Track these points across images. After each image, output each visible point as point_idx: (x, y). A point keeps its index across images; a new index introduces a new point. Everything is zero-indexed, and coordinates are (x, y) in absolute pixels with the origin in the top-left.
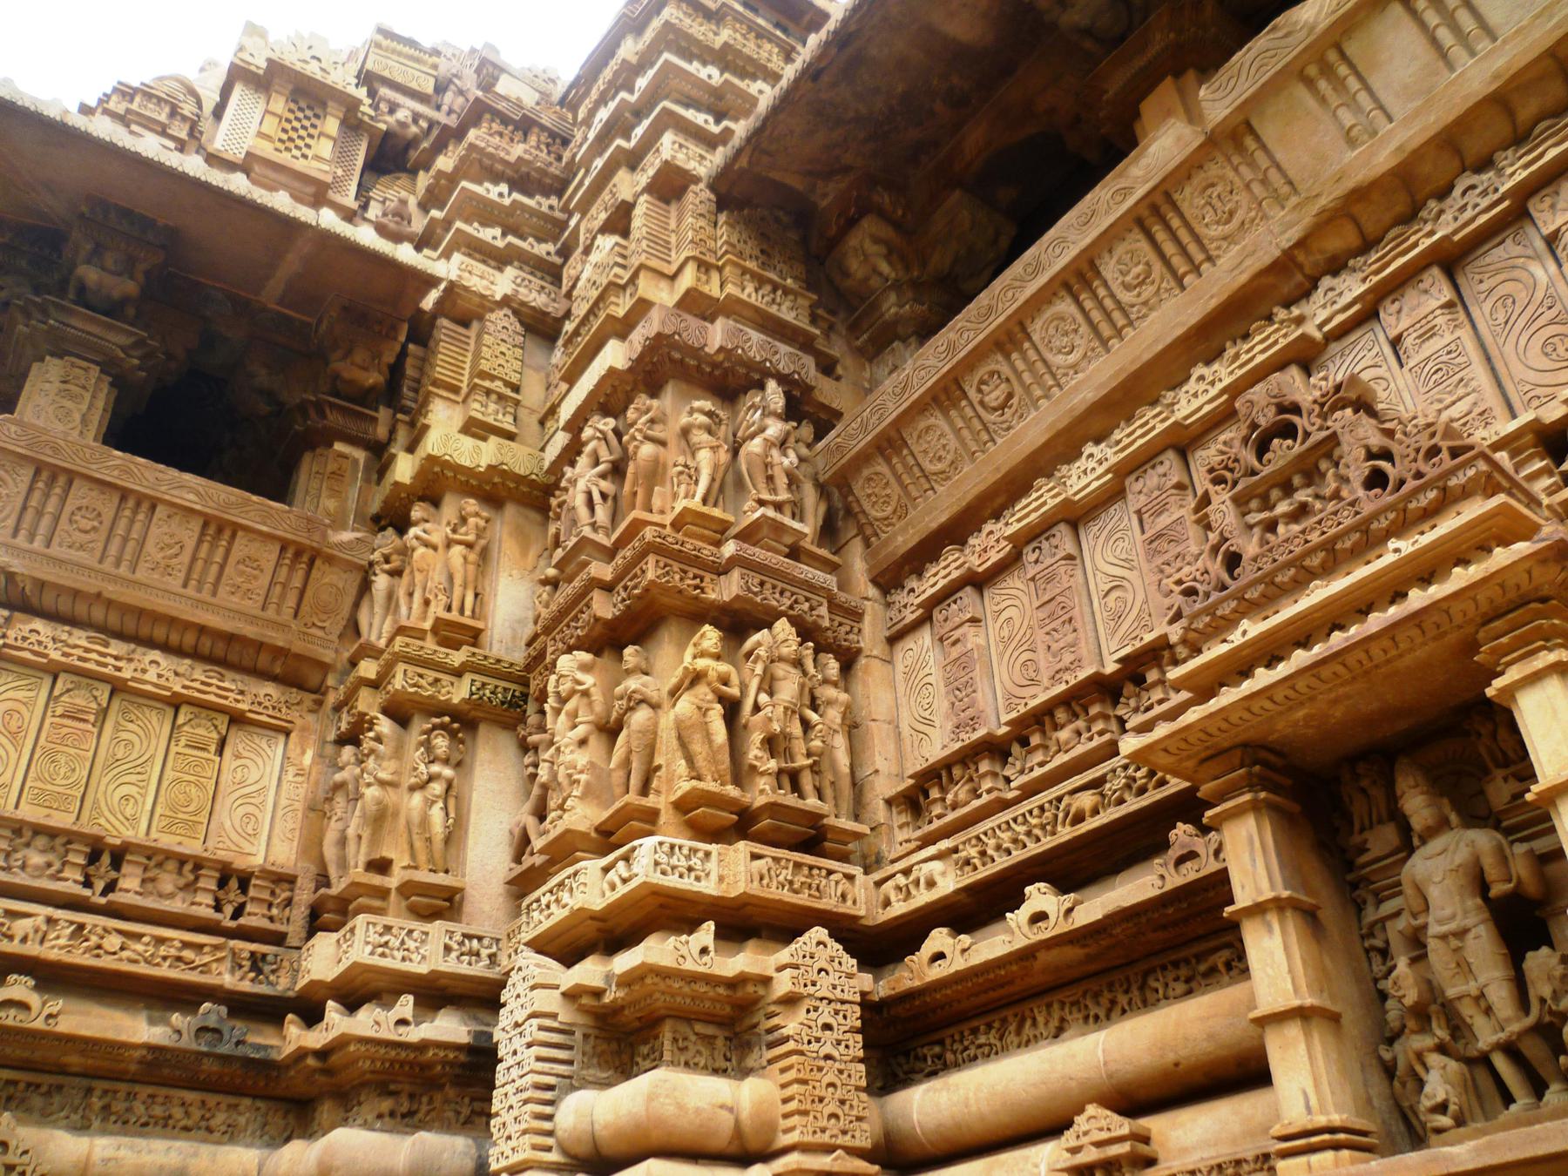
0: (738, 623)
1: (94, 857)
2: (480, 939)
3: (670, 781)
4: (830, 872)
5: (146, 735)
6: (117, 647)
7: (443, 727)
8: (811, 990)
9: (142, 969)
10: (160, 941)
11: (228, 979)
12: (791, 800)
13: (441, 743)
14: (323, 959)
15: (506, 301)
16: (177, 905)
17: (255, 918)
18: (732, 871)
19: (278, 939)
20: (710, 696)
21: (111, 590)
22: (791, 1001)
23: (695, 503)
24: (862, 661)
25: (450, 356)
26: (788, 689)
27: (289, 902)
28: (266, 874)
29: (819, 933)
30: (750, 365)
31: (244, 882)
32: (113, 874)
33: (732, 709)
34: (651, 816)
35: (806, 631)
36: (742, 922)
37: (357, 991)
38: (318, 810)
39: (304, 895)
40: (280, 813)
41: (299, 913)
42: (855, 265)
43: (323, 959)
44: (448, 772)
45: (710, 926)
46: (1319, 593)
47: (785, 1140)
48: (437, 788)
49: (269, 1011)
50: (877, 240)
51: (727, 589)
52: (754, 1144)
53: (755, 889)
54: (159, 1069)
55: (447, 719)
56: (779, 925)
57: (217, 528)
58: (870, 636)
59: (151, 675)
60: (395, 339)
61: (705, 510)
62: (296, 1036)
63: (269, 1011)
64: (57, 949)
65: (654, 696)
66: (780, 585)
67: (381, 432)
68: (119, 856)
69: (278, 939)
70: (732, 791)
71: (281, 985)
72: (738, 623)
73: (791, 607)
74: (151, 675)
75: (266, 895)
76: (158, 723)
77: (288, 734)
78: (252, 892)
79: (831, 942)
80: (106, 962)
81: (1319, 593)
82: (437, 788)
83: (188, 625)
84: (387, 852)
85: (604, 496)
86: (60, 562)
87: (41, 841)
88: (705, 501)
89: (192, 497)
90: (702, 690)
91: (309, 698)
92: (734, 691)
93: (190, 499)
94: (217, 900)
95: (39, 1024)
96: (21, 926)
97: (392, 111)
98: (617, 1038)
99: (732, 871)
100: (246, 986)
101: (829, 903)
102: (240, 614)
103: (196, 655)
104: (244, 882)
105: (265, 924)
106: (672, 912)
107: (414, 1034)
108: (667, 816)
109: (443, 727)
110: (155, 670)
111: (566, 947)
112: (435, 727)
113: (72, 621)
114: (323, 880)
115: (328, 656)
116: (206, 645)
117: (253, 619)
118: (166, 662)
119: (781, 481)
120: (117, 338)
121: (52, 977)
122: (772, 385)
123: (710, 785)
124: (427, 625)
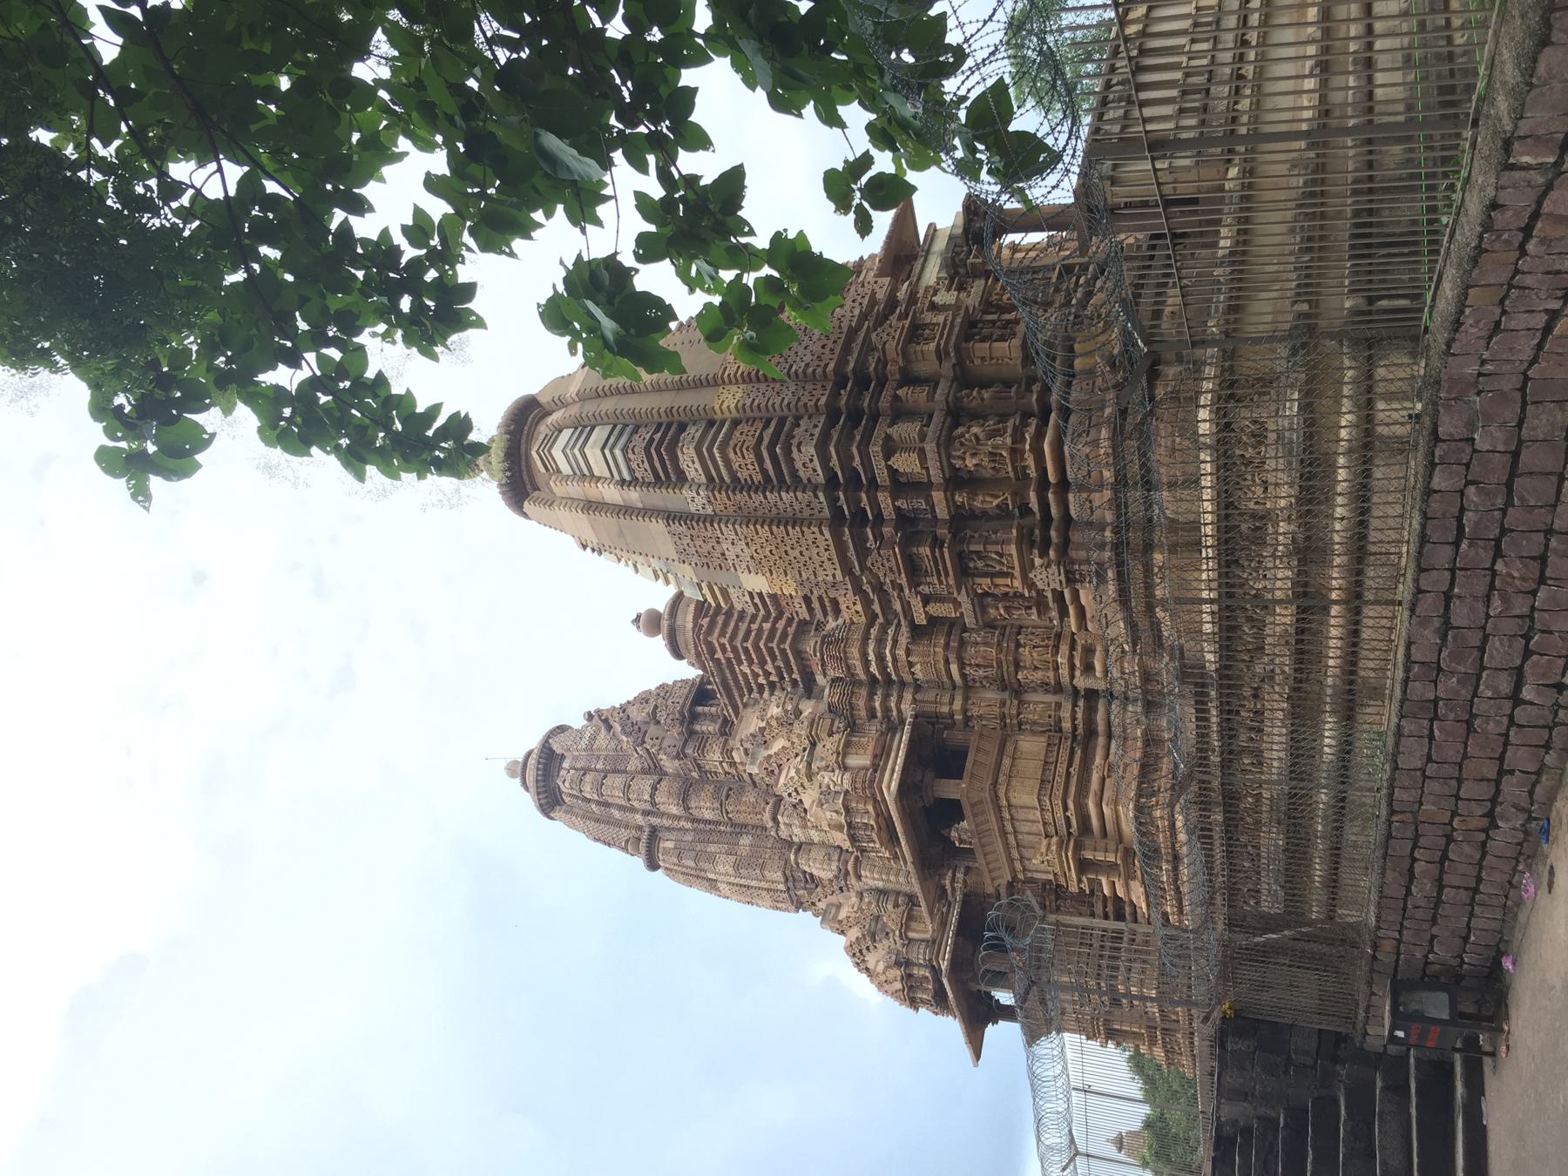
0: (1018, 645)
5: (1020, 763)
14: (1067, 725)
18: (1064, 648)
25: (930, 708)
36: (1073, 648)
37: (1074, 719)
38: (1033, 733)
43: (1067, 725)
51: (1012, 645)
57: (978, 750)
62: (1080, 731)
63: (1074, 737)
72: (1018, 645)
98: (1089, 668)
99: (1064, 648)
106: (1071, 657)
110: (1006, 762)
121: (1070, 765)
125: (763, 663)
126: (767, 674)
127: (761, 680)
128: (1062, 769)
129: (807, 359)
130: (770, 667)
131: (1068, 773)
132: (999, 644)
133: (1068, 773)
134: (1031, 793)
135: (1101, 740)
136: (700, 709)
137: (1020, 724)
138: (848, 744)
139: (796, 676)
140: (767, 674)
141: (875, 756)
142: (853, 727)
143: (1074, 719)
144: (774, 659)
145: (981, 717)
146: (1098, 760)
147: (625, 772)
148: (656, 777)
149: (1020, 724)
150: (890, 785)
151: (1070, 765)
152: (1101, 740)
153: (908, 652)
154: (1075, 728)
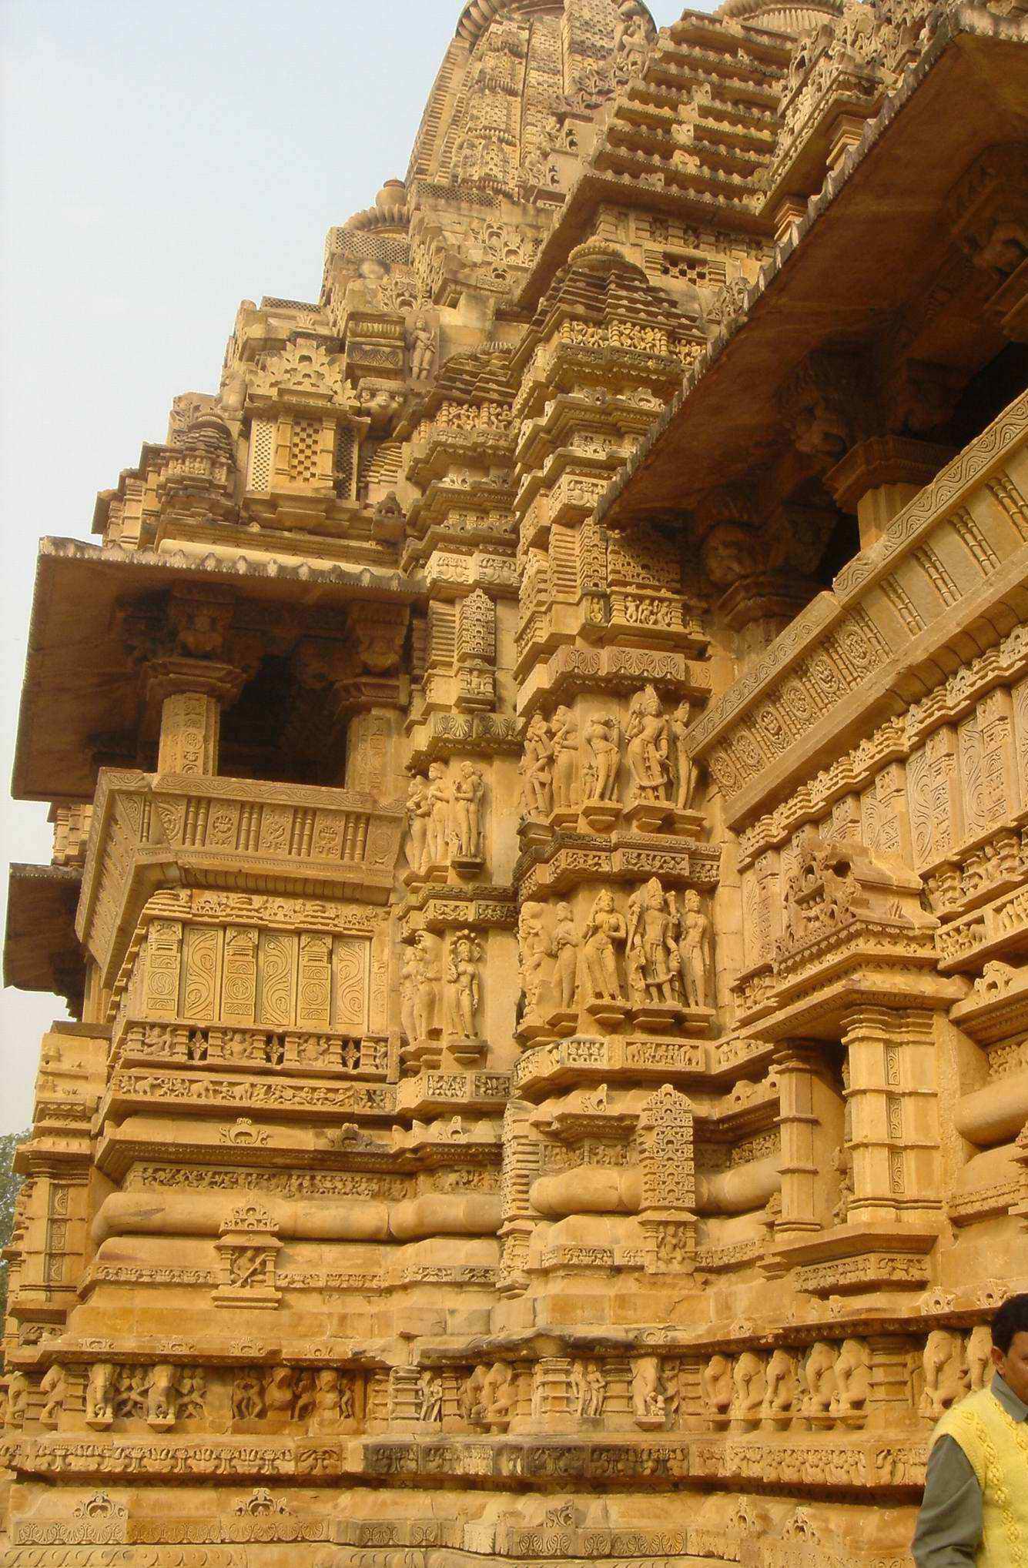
1: (269, 1041)
2: (497, 1079)
3: (583, 997)
4: (681, 1046)
5: (284, 955)
6: (258, 901)
7: (467, 937)
8: (660, 1122)
9: (307, 1107)
10: (314, 1089)
11: (357, 1109)
12: (655, 1004)
13: (464, 948)
14: (409, 1094)
15: (477, 584)
16: (319, 1065)
17: (367, 1068)
19: (382, 1079)
20: (605, 939)
21: (246, 867)
22: (649, 1128)
23: (594, 802)
24: (720, 890)
26: (654, 932)
27: (386, 1055)
28: (371, 1039)
29: (668, 1087)
30: (632, 678)
31: (357, 1043)
32: (281, 1050)
33: (620, 945)
34: (574, 1018)
35: (674, 884)
36: (625, 1080)
37: (429, 1114)
39: (395, 1051)
40: (372, 996)
41: (394, 1060)
42: (713, 563)
44: (470, 968)
45: (605, 1086)
46: (812, 970)
47: (644, 1204)
48: (465, 980)
49: (384, 1122)
50: (726, 545)
52: (631, 1207)
53: (630, 1065)
55: (466, 932)
58: (725, 872)
59: (281, 913)
60: (402, 624)
61: (601, 804)
63: (384, 1122)
64: (258, 1102)
65: (574, 939)
66: (652, 853)
67: (403, 700)
68: (281, 1039)
69: (382, 1079)
70: (620, 1002)
71: (389, 1108)
73: (661, 867)
74: (280, 917)
75: (371, 1052)
76: (290, 944)
77: (370, 939)
78: (363, 1051)
79: (673, 1092)
80: (287, 1106)
81: (831, 959)
82: (465, 980)
83: (296, 880)
84: (436, 1025)
85: (543, 785)
86: (215, 855)
87: (238, 1037)
88: (602, 796)
89: (284, 797)
90: (601, 936)
91: (381, 911)
92: (621, 934)
93: (283, 799)
94: (343, 1058)
95: (258, 1144)
96: (238, 1091)
97: (373, 395)
100: (368, 1111)
101: (680, 1066)
102: (326, 866)
103: (305, 896)
104: (357, 1043)
105: (373, 1070)
107: (462, 1139)
108: (584, 1019)
109: (467, 937)
111: (538, 1092)
112: (460, 938)
113: (227, 888)
114: (404, 1043)
115: (388, 883)
116: (310, 889)
117: (337, 868)
118: (289, 904)
119: (656, 769)
120: (217, 672)
121: (261, 1116)
122: (650, 690)
123: (607, 1001)
124: (448, 863)
131: (229, 1115)
132: (623, 818)
133: (229, 1115)
134: (157, 1003)
135: (369, 1214)
141: (273, 502)
142: (367, 436)
143: (429, 1114)
146: (283, 1208)
151: (261, 1116)
152: (369, 1214)
153: (572, 517)
154: (404, 1121)
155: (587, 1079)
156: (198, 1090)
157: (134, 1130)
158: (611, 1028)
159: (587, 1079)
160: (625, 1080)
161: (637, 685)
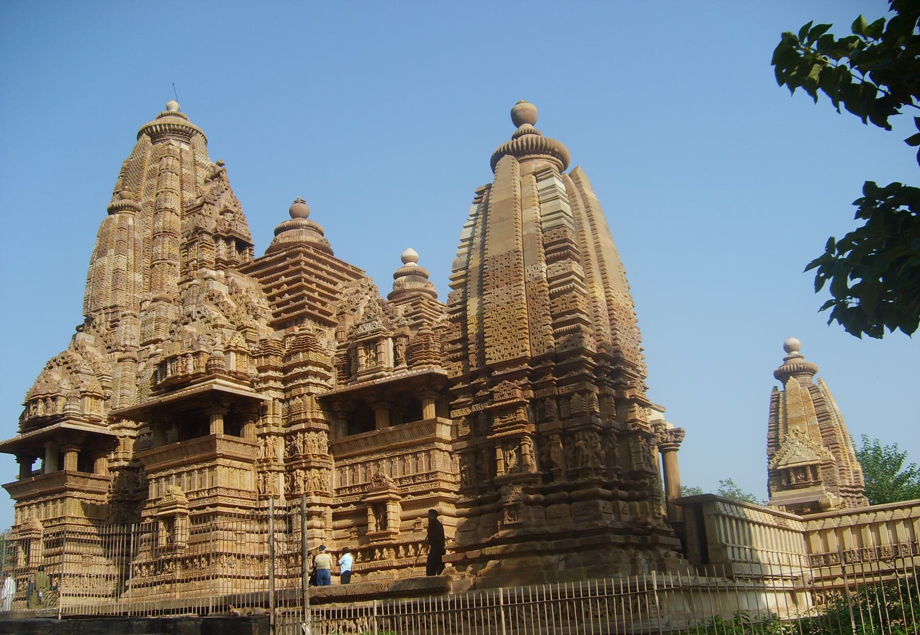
43: (265, 504)
54: (248, 517)
56: (325, 505)
63: (257, 509)
110: (237, 464)
114: (260, 492)
121: (241, 507)
125: (289, 292)
126: (281, 295)
127: (275, 291)
128: (238, 502)
129: (623, 341)
130: (287, 296)
131: (234, 507)
133: (234, 507)
136: (234, 244)
137: (263, 472)
138: (242, 353)
139: (284, 316)
140: (281, 295)
141: (235, 373)
144: (294, 300)
145: (266, 445)
147: (182, 189)
148: (179, 211)
149: (263, 472)
150: (222, 384)
151: (241, 507)
153: (310, 394)
154: (262, 509)
155: (315, 505)
156: (230, 502)
157: (219, 509)
158: (316, 495)
159: (315, 505)
160: (320, 505)
161: (321, 430)
